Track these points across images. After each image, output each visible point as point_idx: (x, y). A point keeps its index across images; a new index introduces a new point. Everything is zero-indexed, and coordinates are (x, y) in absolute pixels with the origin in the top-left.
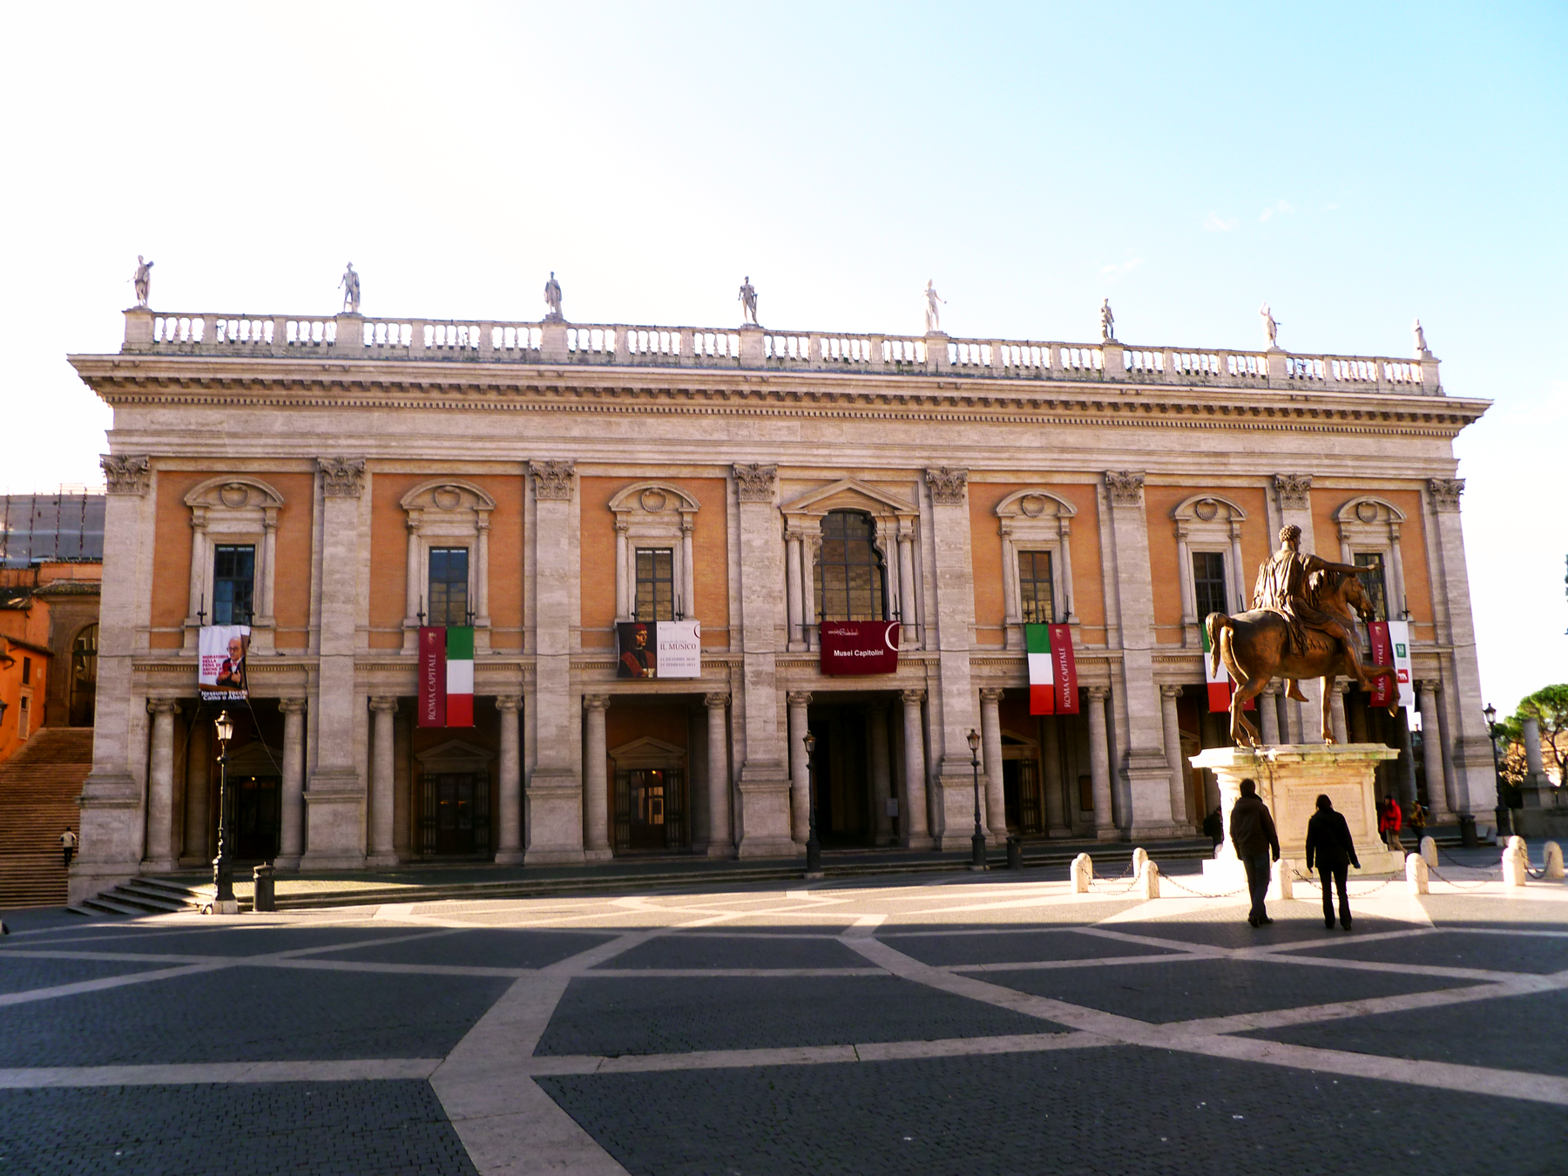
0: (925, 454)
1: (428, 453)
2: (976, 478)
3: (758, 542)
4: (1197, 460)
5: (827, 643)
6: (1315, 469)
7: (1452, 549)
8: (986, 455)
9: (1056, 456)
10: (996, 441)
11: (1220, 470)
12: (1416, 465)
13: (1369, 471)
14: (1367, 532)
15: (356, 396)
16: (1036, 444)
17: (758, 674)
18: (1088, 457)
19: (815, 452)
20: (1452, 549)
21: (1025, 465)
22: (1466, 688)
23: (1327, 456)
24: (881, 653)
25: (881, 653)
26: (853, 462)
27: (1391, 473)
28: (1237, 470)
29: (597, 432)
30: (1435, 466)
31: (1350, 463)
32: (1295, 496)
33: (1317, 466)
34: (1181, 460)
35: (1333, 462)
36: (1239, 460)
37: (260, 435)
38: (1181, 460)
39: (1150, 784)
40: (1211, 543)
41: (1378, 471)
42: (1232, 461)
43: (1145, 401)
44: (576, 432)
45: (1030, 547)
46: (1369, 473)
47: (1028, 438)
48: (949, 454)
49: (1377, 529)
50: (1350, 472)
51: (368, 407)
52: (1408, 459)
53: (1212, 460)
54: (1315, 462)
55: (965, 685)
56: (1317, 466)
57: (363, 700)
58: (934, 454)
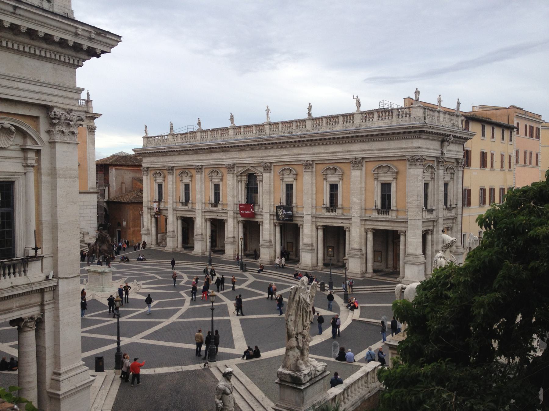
0: (261, 158)
1: (181, 165)
2: (275, 164)
3: (230, 183)
4: (327, 155)
5: (241, 209)
6: (364, 155)
7: (413, 182)
8: (274, 158)
9: (290, 157)
10: (278, 153)
11: (335, 158)
12: (401, 151)
13: (383, 154)
14: (385, 176)
15: (169, 154)
16: (286, 154)
17: (230, 215)
18: (298, 156)
19: (240, 160)
20: (413, 182)
21: (283, 160)
22: (411, 235)
23: (368, 150)
24: (249, 212)
25: (249, 212)
26: (247, 162)
27: (392, 154)
28: (340, 157)
29: (205, 158)
30: (409, 150)
31: (376, 152)
32: (356, 165)
33: (365, 154)
34: (323, 155)
35: (370, 152)
36: (339, 154)
37: (159, 162)
38: (323, 155)
39: (306, 254)
40: (333, 181)
41: (387, 154)
42: (337, 154)
43: (307, 139)
44: (201, 158)
45: (287, 183)
46: (383, 155)
47: (284, 152)
48: (267, 158)
49: (389, 175)
50: (376, 155)
51: (172, 155)
52: (398, 149)
53: (332, 154)
54: (364, 152)
55: (268, 221)
56: (365, 154)
57: (175, 217)
58: (263, 158)
